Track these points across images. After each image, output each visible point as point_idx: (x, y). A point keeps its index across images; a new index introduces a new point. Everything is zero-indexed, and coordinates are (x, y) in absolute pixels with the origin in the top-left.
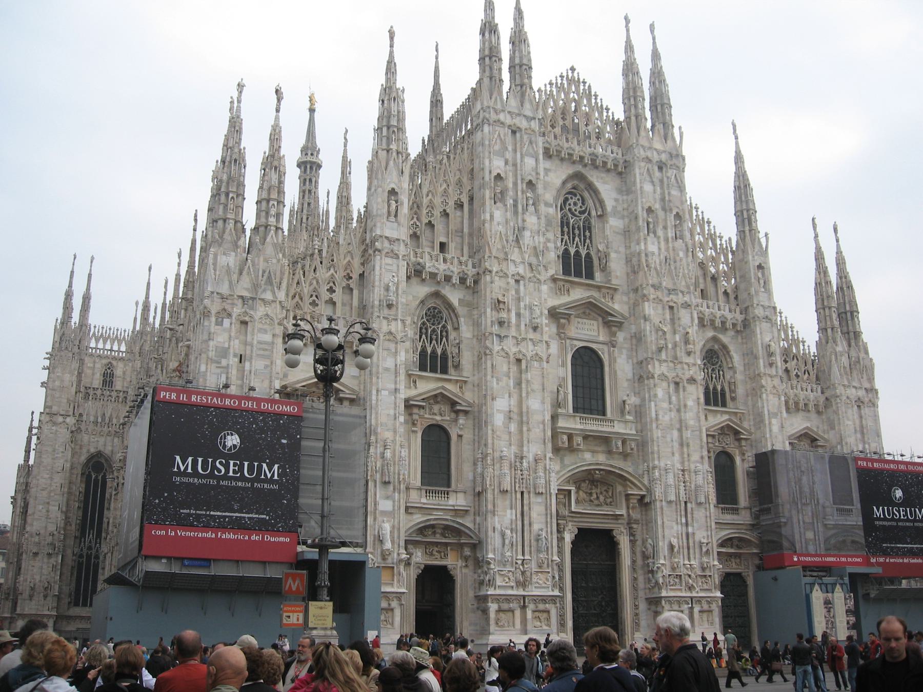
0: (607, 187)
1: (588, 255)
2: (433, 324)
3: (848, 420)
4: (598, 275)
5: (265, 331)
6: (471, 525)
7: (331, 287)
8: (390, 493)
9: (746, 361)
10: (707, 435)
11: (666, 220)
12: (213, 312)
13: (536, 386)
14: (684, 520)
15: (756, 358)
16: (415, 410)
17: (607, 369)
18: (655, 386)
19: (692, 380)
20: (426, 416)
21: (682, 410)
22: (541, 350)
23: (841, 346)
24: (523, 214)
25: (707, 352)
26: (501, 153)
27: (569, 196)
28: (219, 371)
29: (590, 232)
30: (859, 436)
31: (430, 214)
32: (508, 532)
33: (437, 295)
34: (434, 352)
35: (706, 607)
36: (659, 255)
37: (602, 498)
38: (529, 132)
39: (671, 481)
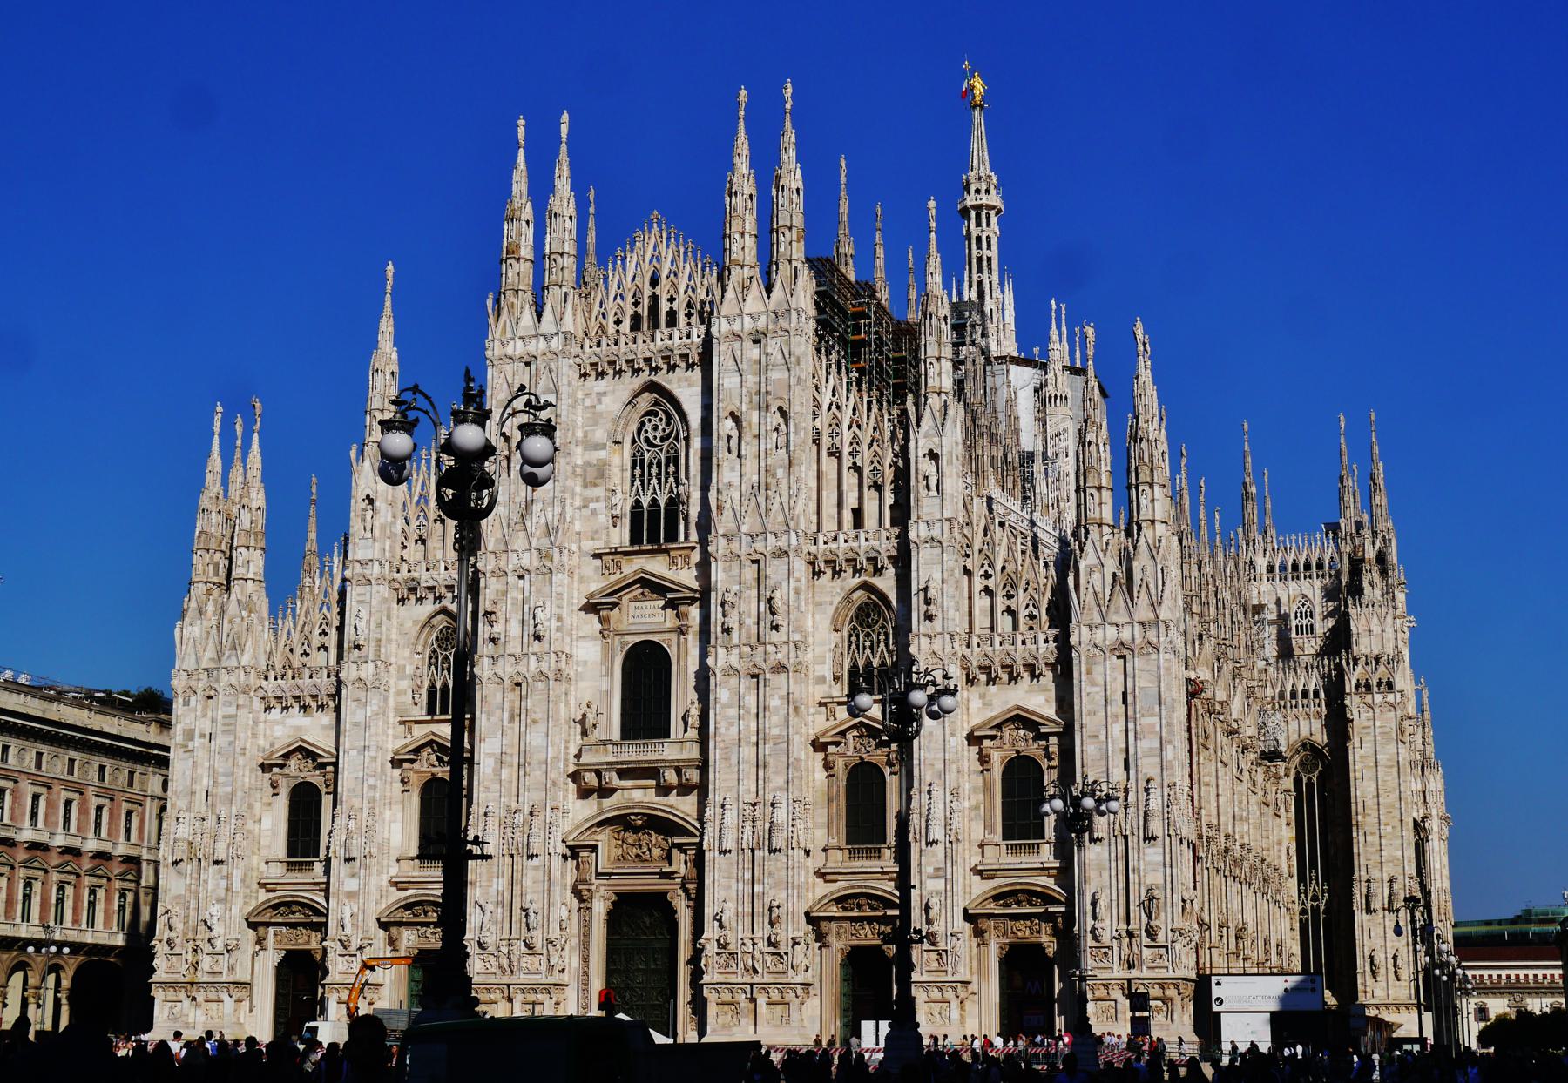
1: (674, 502)
3: (1093, 684)
12: (180, 692)
13: (539, 714)
14: (748, 876)
16: (406, 765)
17: (674, 668)
19: (780, 668)
22: (549, 665)
25: (860, 608)
27: (645, 420)
29: (677, 465)
32: (489, 908)
35: (776, 996)
38: (549, 356)
39: (731, 817)
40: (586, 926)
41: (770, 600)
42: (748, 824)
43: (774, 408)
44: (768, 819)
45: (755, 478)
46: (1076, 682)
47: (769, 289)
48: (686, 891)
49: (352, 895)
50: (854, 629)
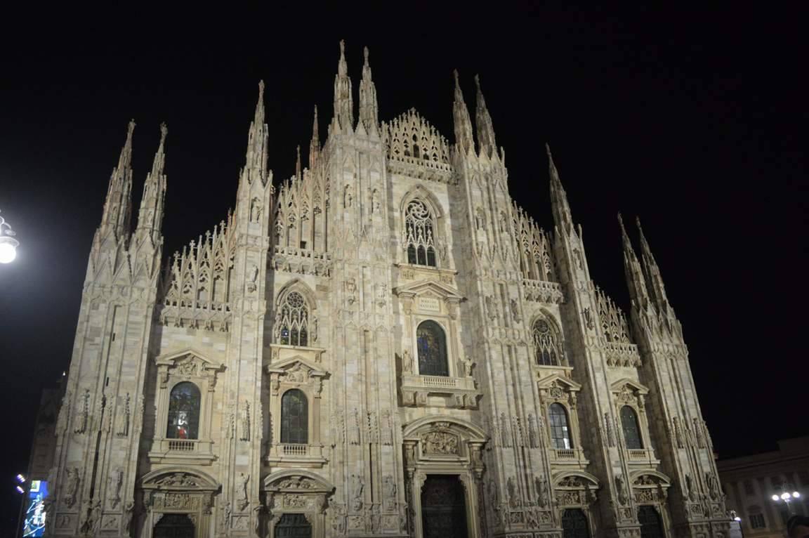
0: (443, 195)
1: (430, 249)
2: (295, 307)
3: (663, 371)
4: (439, 263)
5: (137, 313)
6: (326, 476)
7: (203, 280)
8: (246, 449)
9: (571, 327)
10: (539, 390)
11: (492, 218)
14: (522, 463)
15: (578, 323)
18: (489, 349)
19: (522, 343)
20: (286, 382)
21: (515, 369)
23: (651, 312)
24: (369, 215)
25: (537, 322)
26: (349, 169)
27: (413, 204)
28: (93, 347)
30: (674, 384)
31: (292, 219)
33: (296, 281)
34: (294, 330)
36: (488, 243)
37: (448, 448)
40: (408, 493)
41: (513, 303)
42: (519, 432)
43: (500, 211)
44: (528, 430)
45: (493, 243)
46: (656, 369)
47: (490, 155)
48: (475, 473)
49: (242, 468)
50: (535, 332)
